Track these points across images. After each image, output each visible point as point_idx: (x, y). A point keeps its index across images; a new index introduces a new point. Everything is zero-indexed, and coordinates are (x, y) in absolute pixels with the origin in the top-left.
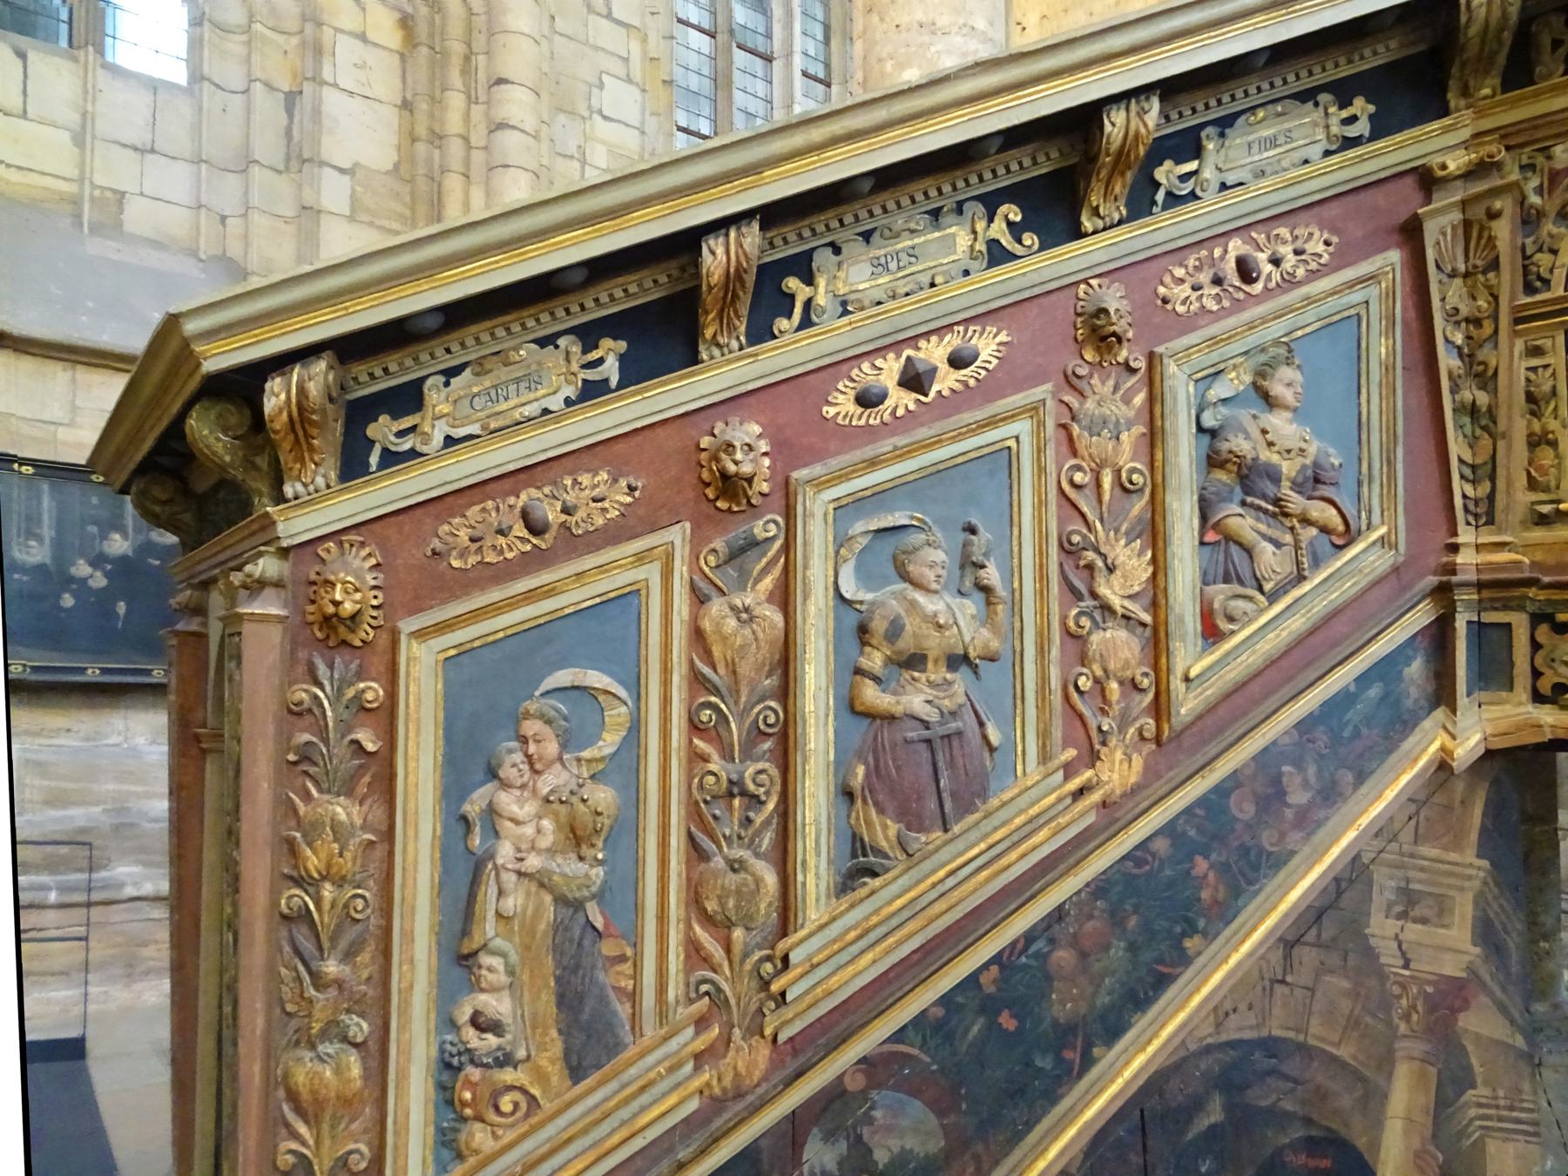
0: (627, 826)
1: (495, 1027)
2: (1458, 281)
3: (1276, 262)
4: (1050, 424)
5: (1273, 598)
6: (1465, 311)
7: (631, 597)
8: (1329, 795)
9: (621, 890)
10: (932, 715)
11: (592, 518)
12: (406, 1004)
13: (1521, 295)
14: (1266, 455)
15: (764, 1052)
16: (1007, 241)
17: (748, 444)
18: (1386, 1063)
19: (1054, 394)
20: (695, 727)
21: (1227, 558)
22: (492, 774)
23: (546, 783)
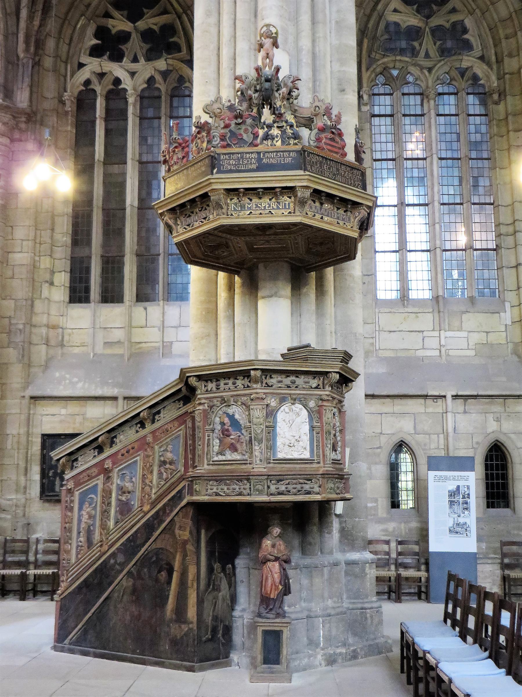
8: (171, 511)
9: (93, 525)
11: (94, 475)
17: (108, 464)
18: (176, 552)
20: (103, 503)
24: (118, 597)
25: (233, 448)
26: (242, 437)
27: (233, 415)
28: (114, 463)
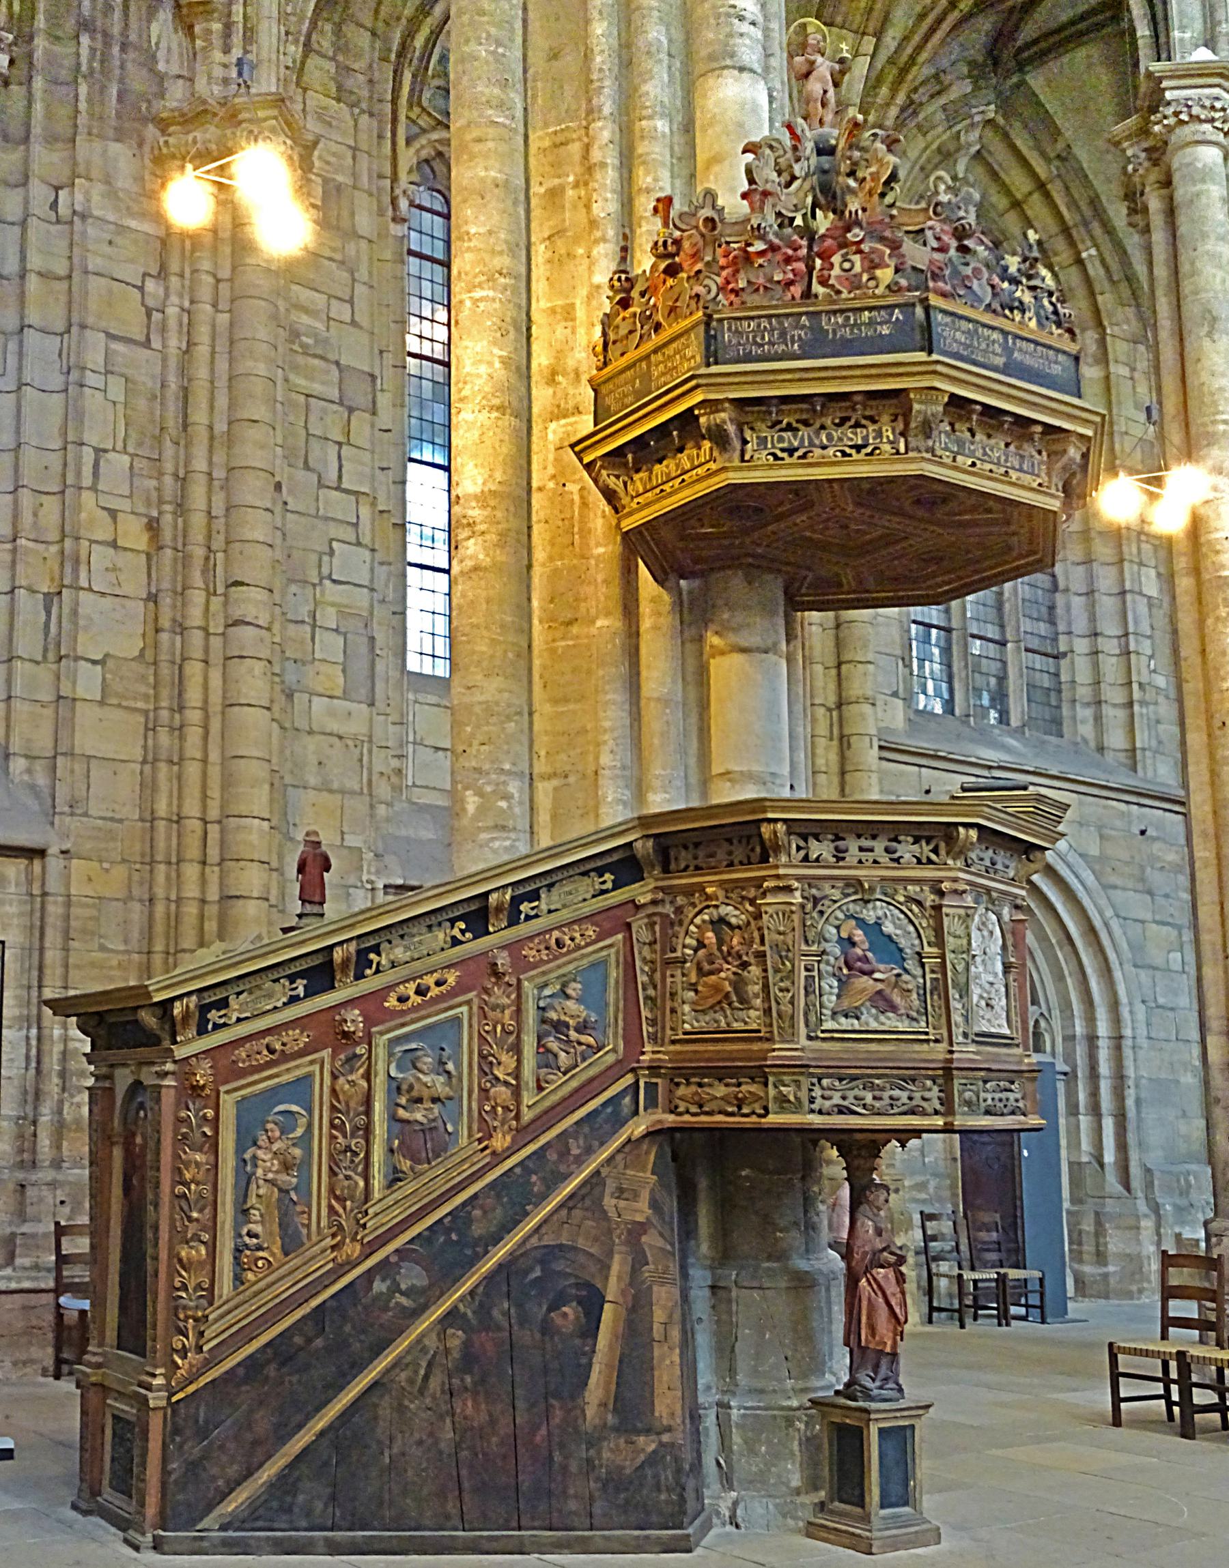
0: (307, 1161)
1: (256, 1236)
3: (572, 939)
4: (475, 1008)
5: (565, 1074)
7: (309, 1077)
9: (304, 1188)
10: (425, 1121)
12: (222, 1229)
14: (563, 1018)
15: (358, 1247)
16: (459, 936)
19: (478, 996)
20: (332, 1126)
21: (546, 1058)
22: (255, 1144)
23: (275, 1147)
24: (411, 1381)
25: (883, 1003)
26: (906, 977)
27: (878, 925)
28: (369, 1021)
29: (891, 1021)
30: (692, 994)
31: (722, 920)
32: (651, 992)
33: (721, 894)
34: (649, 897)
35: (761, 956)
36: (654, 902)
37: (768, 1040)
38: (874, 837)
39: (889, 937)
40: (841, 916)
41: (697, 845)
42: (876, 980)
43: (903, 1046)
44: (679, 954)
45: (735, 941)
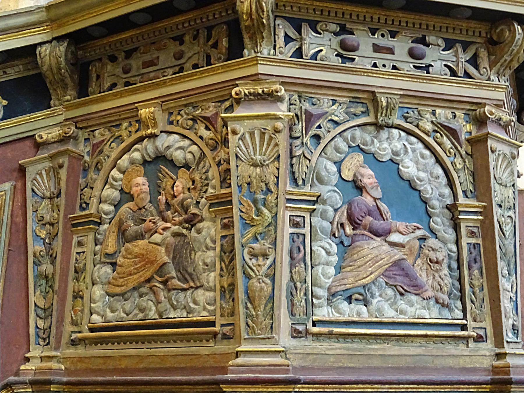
2: (47, 201)
6: (47, 218)
13: (79, 212)
25: (402, 280)
26: (432, 242)
29: (414, 309)
30: (108, 269)
31: (161, 158)
32: (46, 267)
33: (161, 118)
34: (55, 133)
35: (222, 203)
36: (63, 140)
37: (225, 337)
38: (393, 35)
39: (411, 184)
40: (343, 146)
41: (129, 54)
42: (393, 244)
43: (433, 348)
44: (92, 210)
45: (179, 186)
